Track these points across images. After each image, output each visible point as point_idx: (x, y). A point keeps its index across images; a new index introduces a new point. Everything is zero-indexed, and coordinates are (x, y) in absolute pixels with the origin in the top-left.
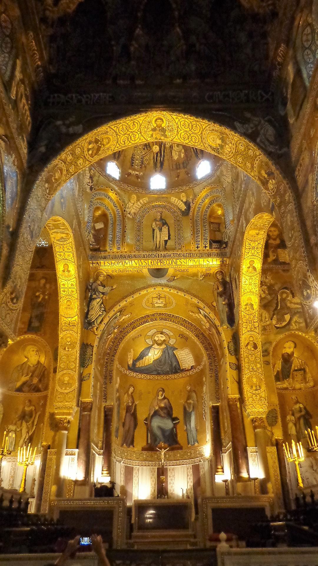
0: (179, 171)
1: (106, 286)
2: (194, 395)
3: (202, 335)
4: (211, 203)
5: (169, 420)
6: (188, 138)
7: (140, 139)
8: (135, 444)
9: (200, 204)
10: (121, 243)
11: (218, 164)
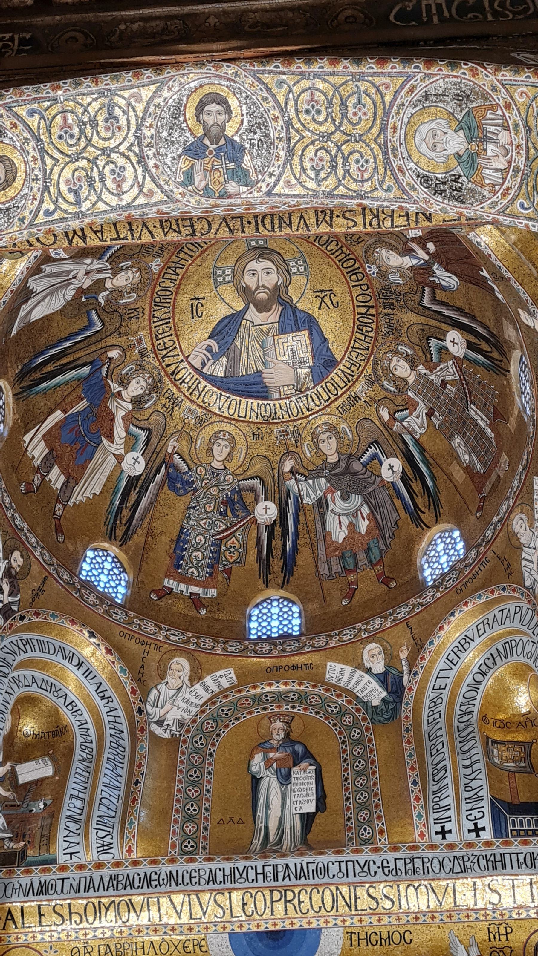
0: (352, 577)
4: (484, 668)
6: (334, 167)
7: (141, 191)
9: (442, 674)
10: (117, 827)
11: (495, 519)
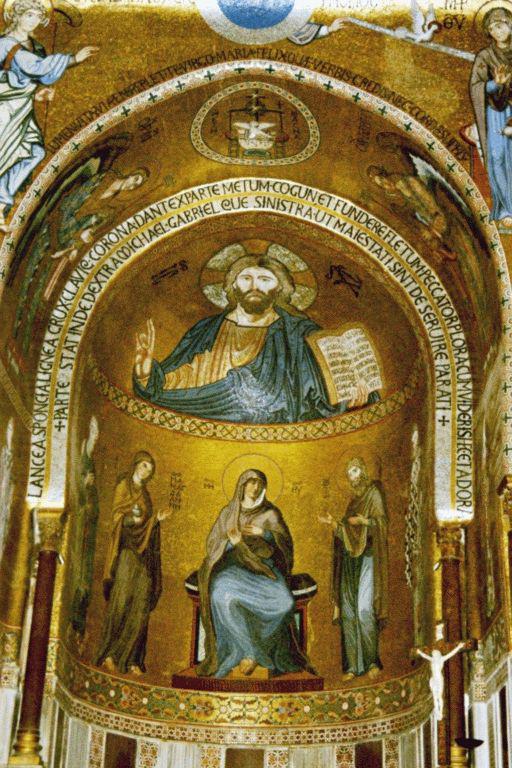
1: (48, 51)
2: (375, 496)
3: (415, 269)
5: (280, 586)
8: (147, 662)
